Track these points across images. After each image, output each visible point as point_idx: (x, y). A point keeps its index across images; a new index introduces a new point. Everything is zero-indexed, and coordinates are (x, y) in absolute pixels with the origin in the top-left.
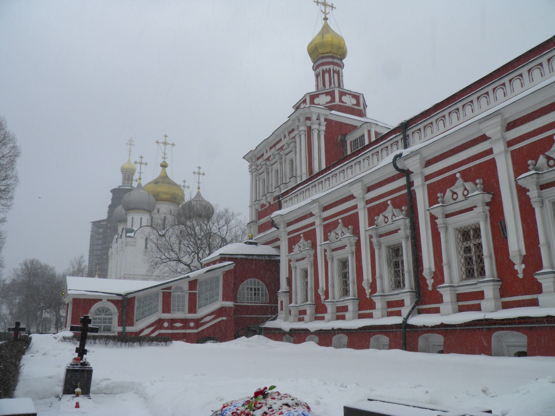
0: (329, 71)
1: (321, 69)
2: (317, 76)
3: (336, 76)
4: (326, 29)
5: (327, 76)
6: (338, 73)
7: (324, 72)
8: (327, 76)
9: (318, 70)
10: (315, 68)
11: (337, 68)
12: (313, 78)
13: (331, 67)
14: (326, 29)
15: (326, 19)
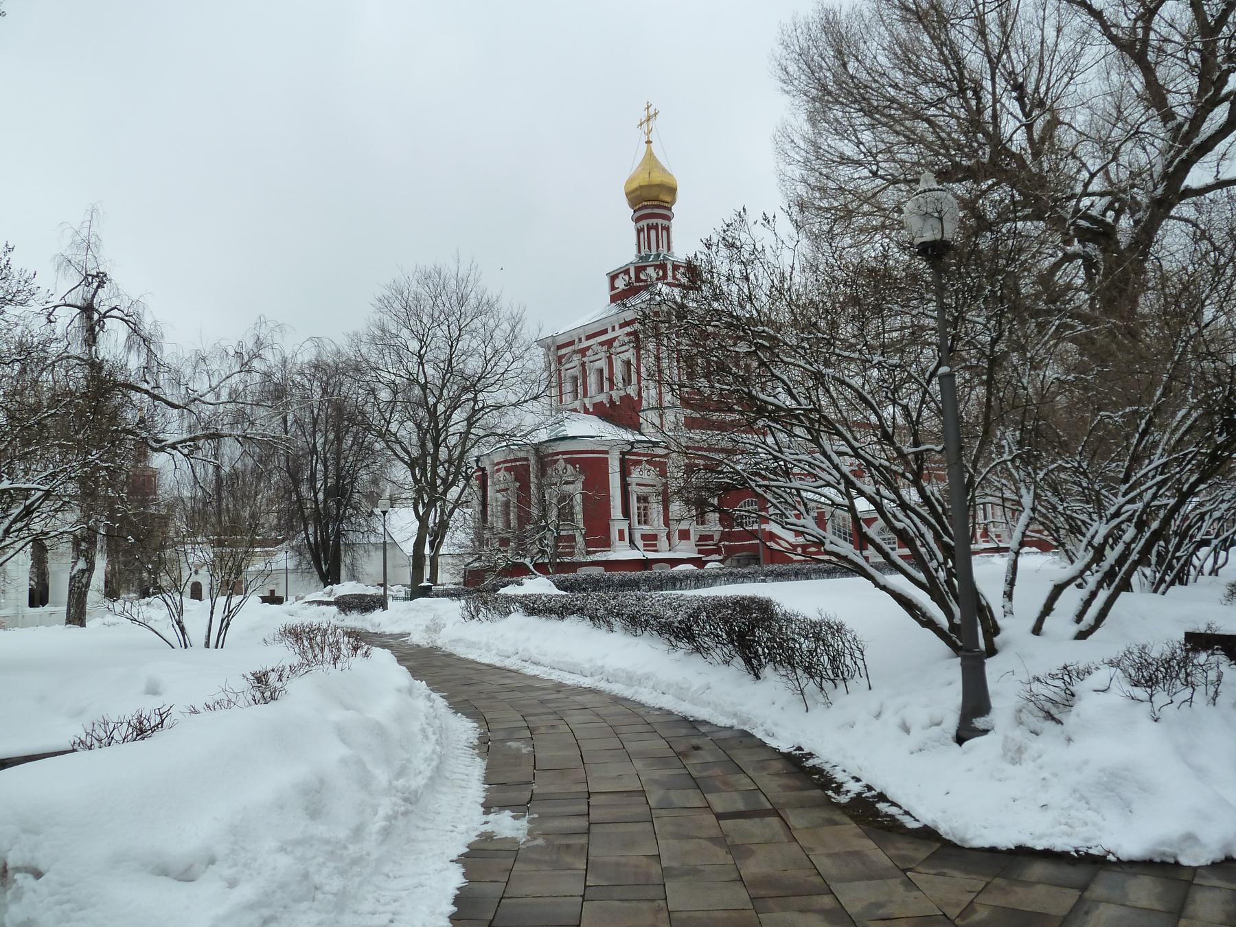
0: (656, 227)
1: (644, 223)
2: (639, 231)
3: (665, 233)
4: (650, 158)
5: (653, 233)
6: (667, 229)
7: (649, 228)
8: (653, 233)
9: (641, 224)
10: (637, 220)
11: (665, 222)
12: (634, 233)
13: (660, 222)
14: (650, 158)
15: (649, 142)
